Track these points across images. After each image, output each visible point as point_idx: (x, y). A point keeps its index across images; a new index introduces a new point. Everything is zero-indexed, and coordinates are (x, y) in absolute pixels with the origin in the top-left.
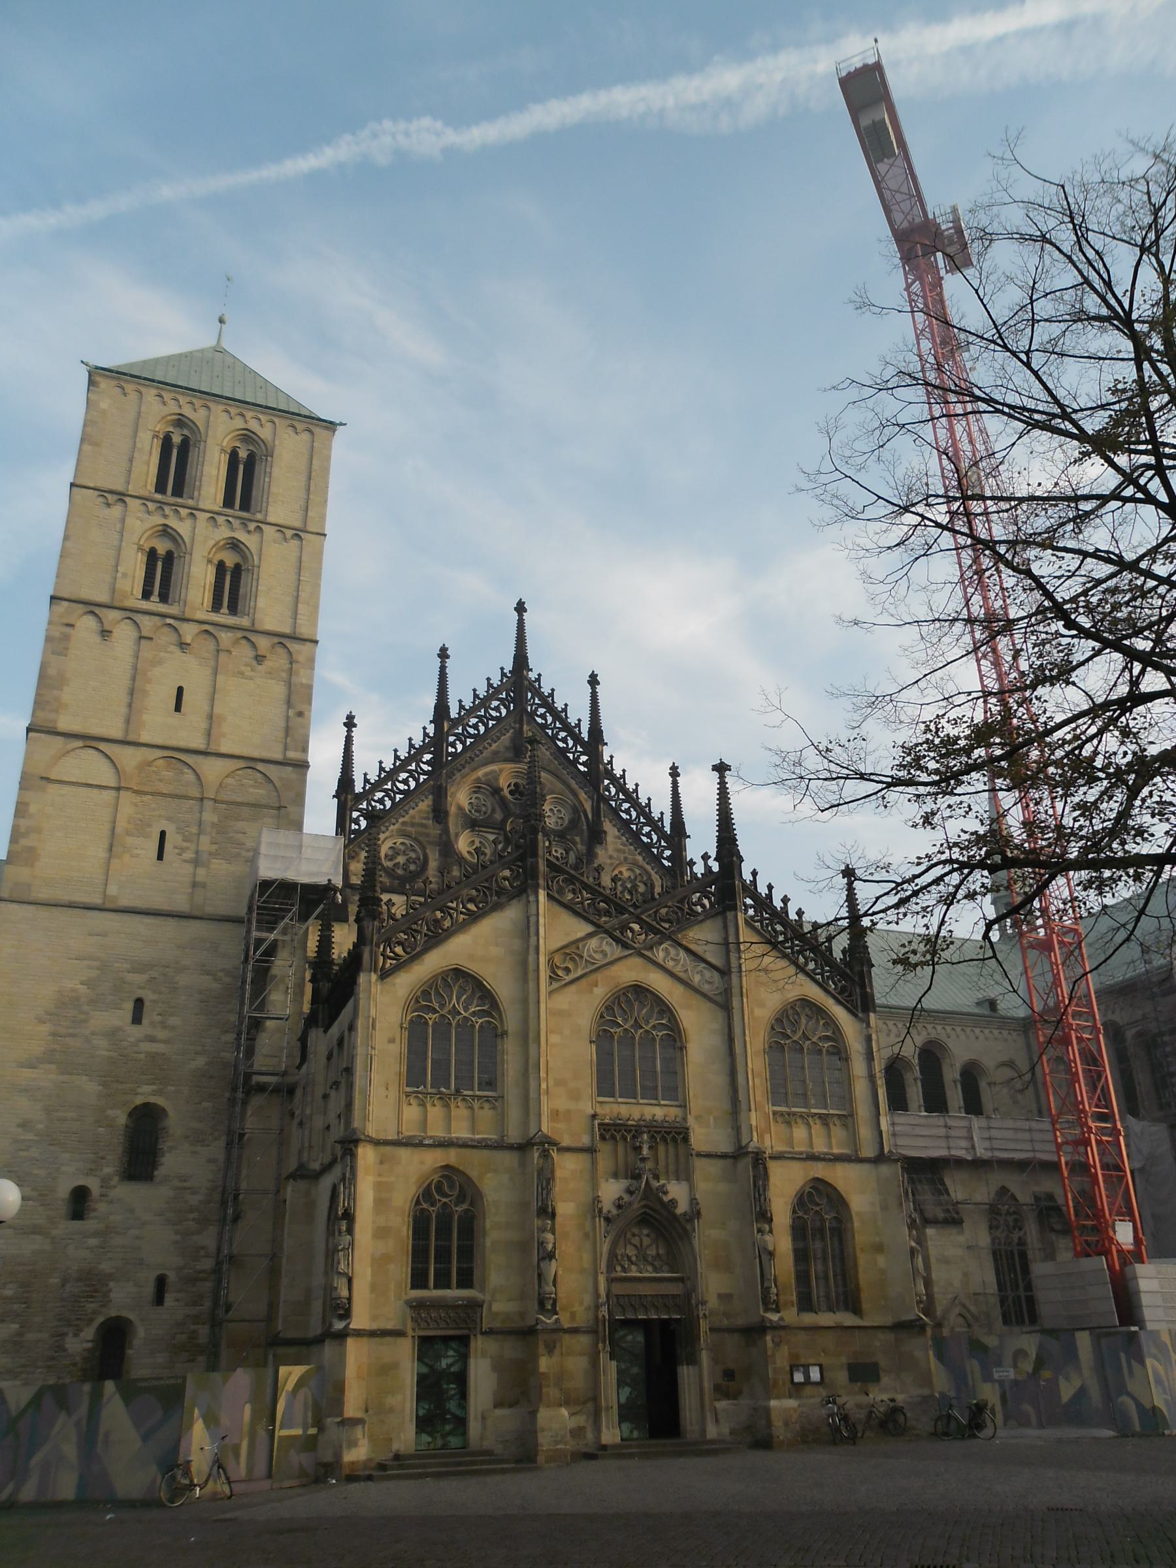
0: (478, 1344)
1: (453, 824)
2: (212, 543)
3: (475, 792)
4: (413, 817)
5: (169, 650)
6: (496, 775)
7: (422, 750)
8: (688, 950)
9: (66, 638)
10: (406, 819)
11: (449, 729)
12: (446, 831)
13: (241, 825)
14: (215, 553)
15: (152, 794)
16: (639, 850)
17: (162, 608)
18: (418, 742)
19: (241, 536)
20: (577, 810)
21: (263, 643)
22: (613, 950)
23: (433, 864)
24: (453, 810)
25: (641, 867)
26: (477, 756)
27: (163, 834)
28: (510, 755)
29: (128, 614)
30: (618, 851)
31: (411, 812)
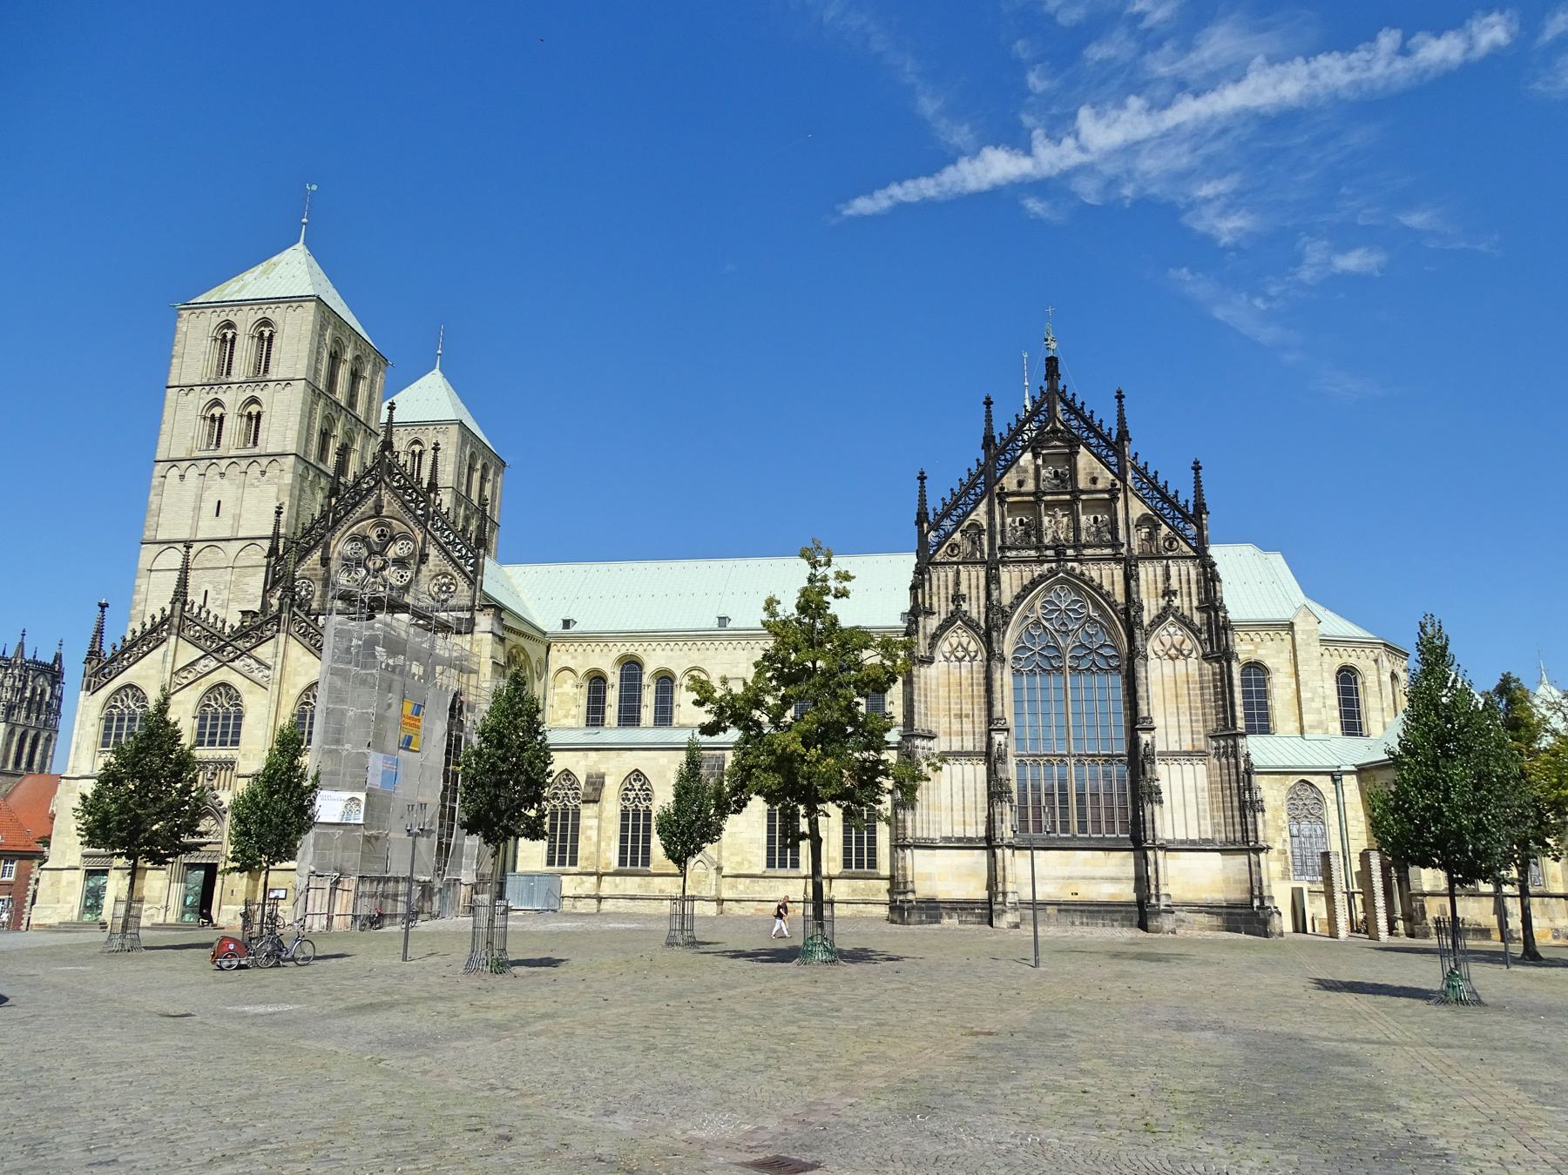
0: (112, 873)
1: (335, 565)
7: (318, 522)
8: (257, 660)
10: (305, 567)
12: (328, 571)
13: (246, 580)
15: (202, 569)
17: (211, 454)
19: (257, 393)
20: (415, 542)
21: (264, 461)
22: (213, 664)
24: (336, 555)
25: (451, 575)
27: (206, 592)
28: (373, 513)
29: (193, 462)
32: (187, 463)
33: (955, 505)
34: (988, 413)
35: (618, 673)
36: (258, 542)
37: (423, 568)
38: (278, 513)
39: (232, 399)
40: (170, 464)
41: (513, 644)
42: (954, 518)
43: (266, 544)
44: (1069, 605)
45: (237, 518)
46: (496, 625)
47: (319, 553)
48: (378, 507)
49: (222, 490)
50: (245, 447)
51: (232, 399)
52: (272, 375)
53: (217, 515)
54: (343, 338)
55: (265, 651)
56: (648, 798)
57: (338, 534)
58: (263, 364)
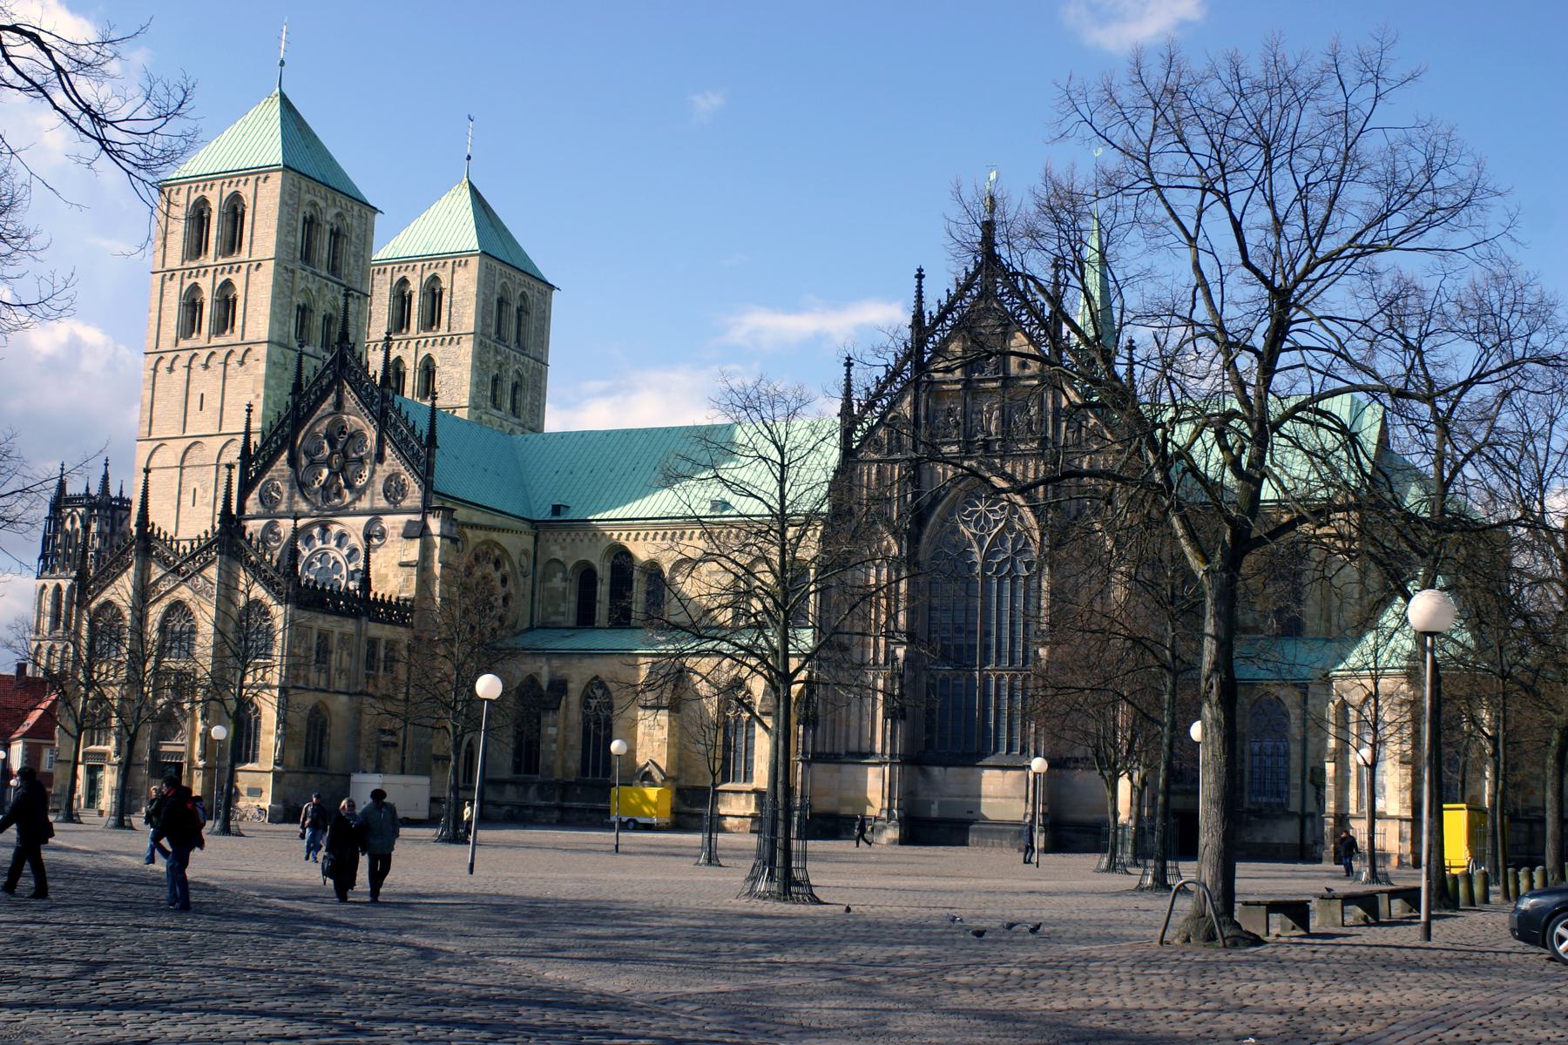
0: (108, 768)
7: (284, 421)
18: (284, 414)
30: (390, 465)
32: (173, 355)
33: (879, 394)
34: (920, 287)
35: (609, 564)
36: (237, 437)
37: (378, 467)
38: (249, 411)
39: (207, 285)
40: (157, 356)
41: (478, 540)
42: (878, 410)
44: (990, 506)
46: (447, 526)
47: (286, 454)
48: (339, 405)
49: (206, 382)
51: (207, 285)
52: (244, 255)
54: (318, 200)
55: (212, 572)
56: (610, 707)
57: (302, 433)
58: (232, 243)
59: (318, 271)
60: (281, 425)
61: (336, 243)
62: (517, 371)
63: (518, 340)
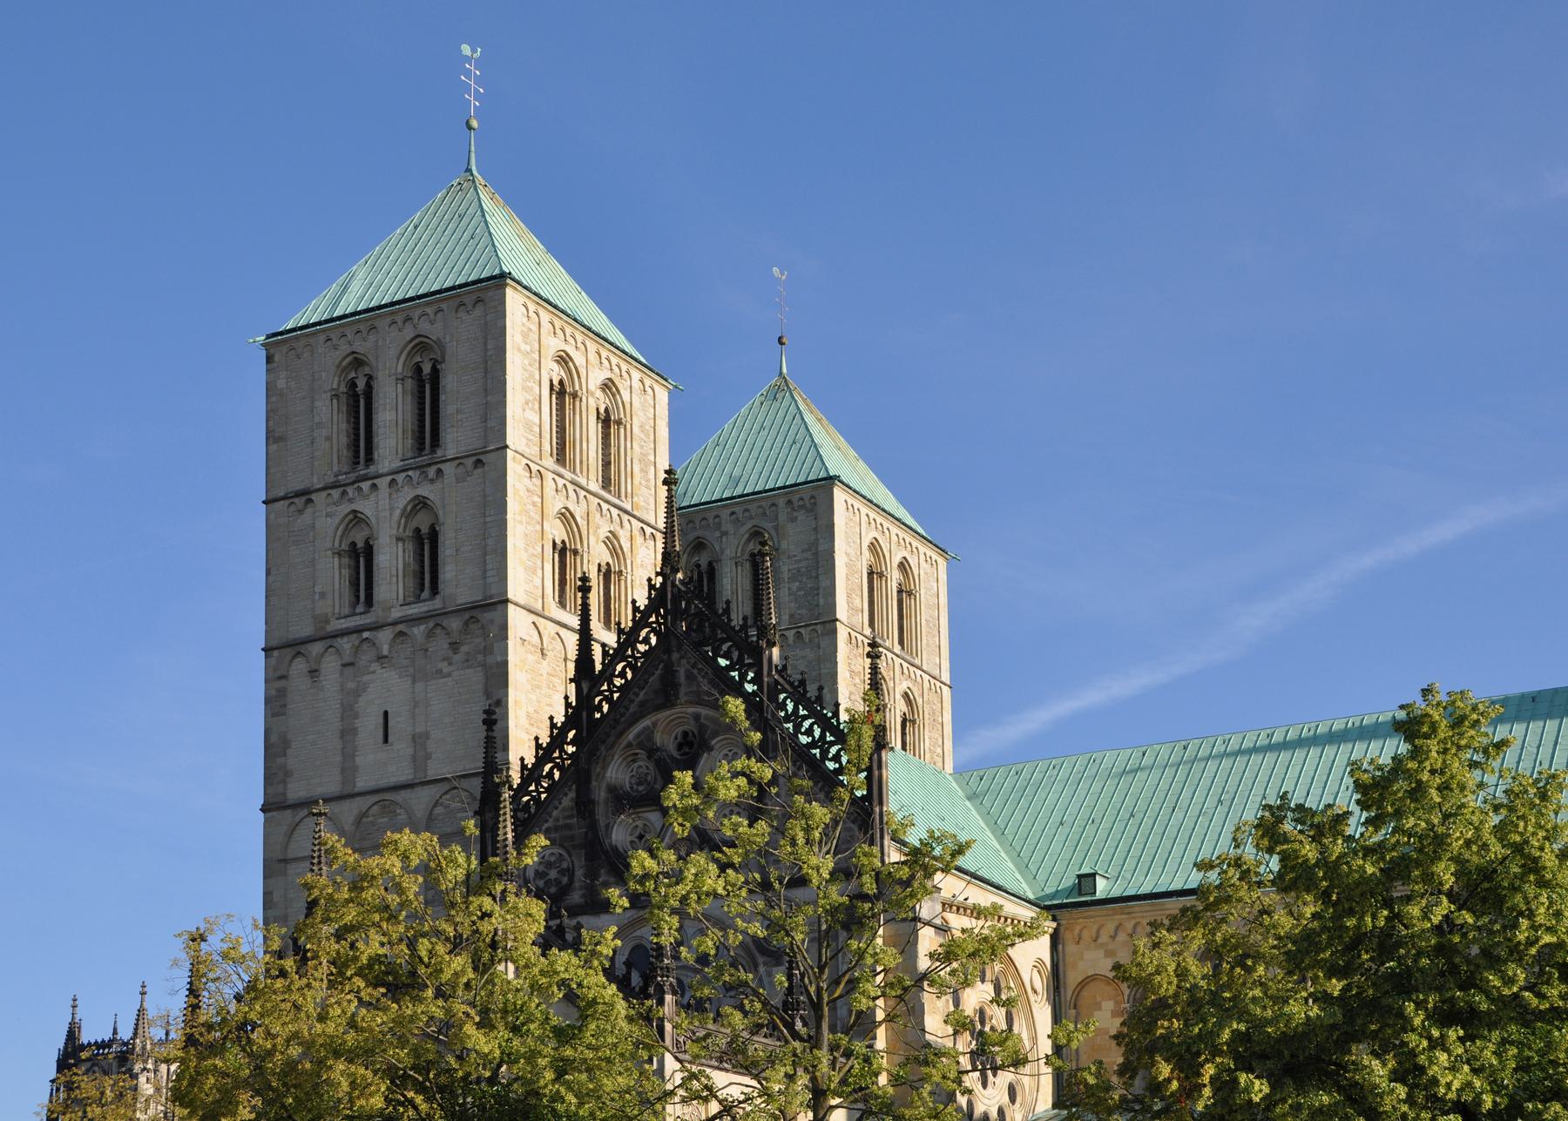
2: (398, 512)
3: (634, 761)
4: (557, 819)
5: (371, 669)
6: (648, 734)
9: (282, 693)
11: (590, 690)
12: (593, 826)
14: (406, 523)
16: (820, 785)
18: (560, 719)
21: (455, 624)
23: (579, 873)
24: (600, 794)
26: (623, 715)
29: (329, 642)
31: (555, 813)
32: (316, 648)
40: (290, 652)
43: (476, 785)
45: (419, 740)
47: (572, 795)
50: (418, 599)
53: (386, 740)
59: (583, 481)
60: (558, 738)
61: (606, 437)
62: (906, 696)
63: (901, 642)
